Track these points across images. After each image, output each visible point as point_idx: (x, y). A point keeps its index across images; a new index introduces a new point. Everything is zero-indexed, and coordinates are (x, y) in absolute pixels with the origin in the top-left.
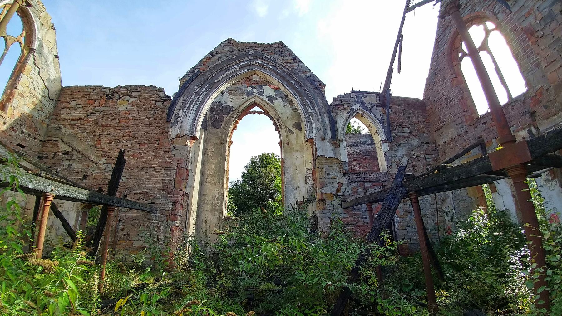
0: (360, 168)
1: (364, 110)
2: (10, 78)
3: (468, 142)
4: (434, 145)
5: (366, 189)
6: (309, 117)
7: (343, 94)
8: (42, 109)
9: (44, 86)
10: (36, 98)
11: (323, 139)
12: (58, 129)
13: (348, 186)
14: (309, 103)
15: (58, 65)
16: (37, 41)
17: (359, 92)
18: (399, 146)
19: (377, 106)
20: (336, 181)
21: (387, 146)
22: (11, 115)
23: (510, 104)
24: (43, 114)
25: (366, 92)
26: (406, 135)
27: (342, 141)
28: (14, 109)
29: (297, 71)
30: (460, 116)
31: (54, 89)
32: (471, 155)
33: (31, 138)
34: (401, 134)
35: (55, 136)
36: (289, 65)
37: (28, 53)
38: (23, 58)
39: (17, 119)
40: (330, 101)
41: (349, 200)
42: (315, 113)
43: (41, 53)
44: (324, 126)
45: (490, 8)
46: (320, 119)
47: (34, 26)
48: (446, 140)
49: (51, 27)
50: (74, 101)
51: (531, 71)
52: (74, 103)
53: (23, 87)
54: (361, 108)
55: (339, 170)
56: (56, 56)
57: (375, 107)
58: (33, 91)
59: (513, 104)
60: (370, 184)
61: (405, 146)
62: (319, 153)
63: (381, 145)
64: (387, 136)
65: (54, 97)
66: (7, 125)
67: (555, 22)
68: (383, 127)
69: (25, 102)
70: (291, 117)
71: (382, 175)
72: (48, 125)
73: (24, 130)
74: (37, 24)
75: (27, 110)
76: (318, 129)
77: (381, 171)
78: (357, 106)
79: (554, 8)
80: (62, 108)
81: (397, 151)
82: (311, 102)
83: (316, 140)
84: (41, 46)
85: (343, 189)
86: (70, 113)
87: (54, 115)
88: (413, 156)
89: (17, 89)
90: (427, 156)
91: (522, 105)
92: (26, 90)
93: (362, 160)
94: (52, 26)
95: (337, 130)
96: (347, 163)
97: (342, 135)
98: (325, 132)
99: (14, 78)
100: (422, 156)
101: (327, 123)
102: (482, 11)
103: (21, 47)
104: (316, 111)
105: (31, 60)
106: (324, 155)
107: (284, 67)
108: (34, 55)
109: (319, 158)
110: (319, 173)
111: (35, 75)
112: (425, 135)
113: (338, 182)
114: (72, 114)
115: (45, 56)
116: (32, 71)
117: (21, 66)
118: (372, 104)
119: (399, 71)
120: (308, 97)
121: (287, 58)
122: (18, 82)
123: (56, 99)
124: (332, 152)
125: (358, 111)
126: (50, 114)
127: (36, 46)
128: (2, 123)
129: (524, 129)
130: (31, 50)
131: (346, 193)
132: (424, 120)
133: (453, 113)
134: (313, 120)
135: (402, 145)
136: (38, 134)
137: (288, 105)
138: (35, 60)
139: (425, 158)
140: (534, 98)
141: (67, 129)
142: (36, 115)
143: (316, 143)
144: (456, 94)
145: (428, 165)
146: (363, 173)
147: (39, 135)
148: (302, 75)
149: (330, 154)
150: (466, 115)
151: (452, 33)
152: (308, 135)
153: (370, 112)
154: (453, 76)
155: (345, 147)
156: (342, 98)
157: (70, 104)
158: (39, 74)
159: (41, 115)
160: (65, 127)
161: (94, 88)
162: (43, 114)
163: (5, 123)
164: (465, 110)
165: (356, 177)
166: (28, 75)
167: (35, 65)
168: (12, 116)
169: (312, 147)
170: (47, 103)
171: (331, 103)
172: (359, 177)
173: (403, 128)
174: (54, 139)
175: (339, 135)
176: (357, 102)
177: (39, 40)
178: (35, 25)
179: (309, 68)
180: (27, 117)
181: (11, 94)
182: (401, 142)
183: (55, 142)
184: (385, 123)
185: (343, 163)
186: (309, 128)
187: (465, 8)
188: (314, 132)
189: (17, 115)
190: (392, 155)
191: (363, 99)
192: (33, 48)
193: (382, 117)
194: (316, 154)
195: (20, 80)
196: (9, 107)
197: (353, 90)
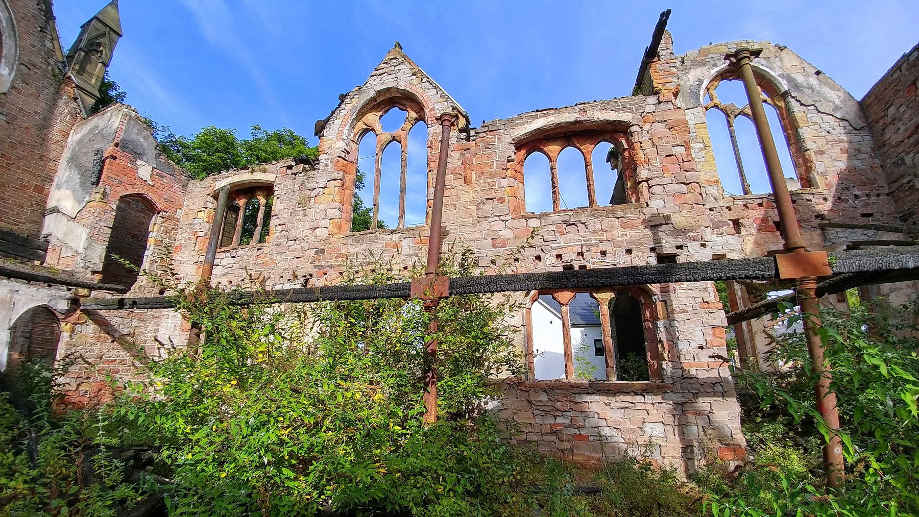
2: (789, 145)
8: (860, 151)
9: (838, 120)
10: (841, 142)
12: (900, 163)
15: (830, 81)
16: (780, 79)
22: (827, 185)
24: (865, 156)
28: (824, 175)
31: (851, 111)
33: (873, 198)
35: (903, 176)
37: (785, 102)
38: (784, 112)
39: (838, 185)
43: (797, 87)
47: (761, 69)
49: (779, 51)
50: (889, 107)
52: (892, 111)
53: (815, 142)
56: (818, 73)
58: (829, 137)
65: (861, 124)
66: (830, 199)
69: (831, 157)
72: (882, 166)
73: (857, 193)
74: (762, 65)
75: (842, 165)
80: (883, 130)
84: (790, 80)
86: (899, 129)
87: (879, 146)
89: (809, 150)
92: (821, 143)
94: (779, 48)
99: (793, 141)
103: (769, 104)
105: (795, 106)
108: (793, 97)
111: (816, 118)
114: (903, 128)
115: (805, 85)
116: (809, 116)
117: (789, 122)
122: (804, 141)
123: (865, 125)
126: (873, 149)
127: (784, 86)
128: (822, 201)
130: (785, 95)
136: (878, 187)
138: (799, 101)
141: (911, 155)
142: (857, 163)
147: (882, 187)
157: (889, 116)
158: (819, 112)
159: (863, 159)
160: (908, 154)
161: (898, 67)
162: (865, 156)
163: (825, 199)
166: (808, 125)
167: (805, 106)
168: (828, 186)
170: (859, 138)
174: (905, 180)
177: (779, 76)
178: (761, 67)
180: (849, 173)
181: (806, 161)
183: (909, 185)
189: (834, 181)
192: (783, 91)
195: (802, 137)
196: (817, 177)
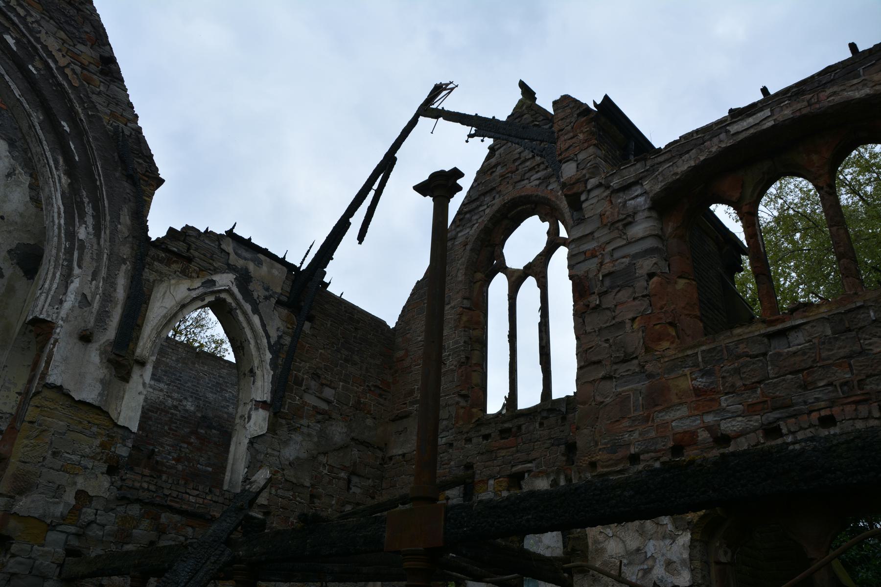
0: (178, 460)
1: (239, 296)
3: (445, 469)
4: (380, 454)
5: (161, 531)
6: (69, 252)
7: (202, 230)
11: (86, 338)
13: (107, 510)
14: (89, 209)
17: (247, 244)
18: (295, 429)
19: (279, 303)
20: (75, 483)
21: (265, 419)
23: (540, 412)
25: (265, 252)
26: (324, 406)
27: (142, 364)
29: (94, 98)
34: (311, 400)
36: (78, 69)
40: (156, 230)
41: (95, 552)
42: (95, 246)
44: (108, 298)
46: (103, 273)
54: (235, 290)
55: (98, 450)
57: (273, 301)
59: (545, 414)
60: (177, 518)
61: (309, 435)
62: (54, 377)
63: (249, 413)
64: (274, 392)
67: (631, 290)
68: (274, 364)
70: (18, 219)
71: (221, 500)
76: (84, 301)
77: (225, 487)
78: (225, 280)
79: (640, 262)
81: (286, 443)
82: (96, 208)
83: (61, 332)
85: (88, 513)
88: (321, 469)
90: (355, 479)
91: (560, 421)
93: (193, 440)
95: (140, 327)
96: (132, 436)
97: (149, 345)
98: (103, 317)
100: (343, 475)
101: (120, 293)
104: (99, 244)
106: (69, 386)
107: (61, 69)
109: (47, 393)
110: (26, 442)
112: (369, 422)
113: (79, 486)
118: (267, 289)
119: (361, 238)
120: (94, 191)
121: (80, 47)
124: (98, 388)
125: (223, 295)
129: (548, 475)
131: (95, 531)
132: (379, 383)
134: (80, 267)
135: (305, 430)
137: (25, 180)
139: (349, 481)
143: (56, 341)
145: (349, 503)
146: (170, 481)
148: (106, 119)
149: (89, 394)
150: (461, 404)
151: (495, 208)
152: (40, 306)
153: (256, 311)
154: (466, 303)
155: (144, 384)
156: (194, 239)
164: (463, 392)
165: (145, 485)
169: (41, 349)
171: (158, 239)
172: (152, 488)
173: (322, 385)
175: (141, 344)
176: (231, 268)
179: (137, 111)
182: (304, 422)
184: (283, 356)
185: (120, 431)
186: (55, 286)
187: (534, 172)
188: (67, 305)
190: (269, 451)
191: (251, 267)
193: (280, 337)
194: (44, 375)
197: (235, 231)
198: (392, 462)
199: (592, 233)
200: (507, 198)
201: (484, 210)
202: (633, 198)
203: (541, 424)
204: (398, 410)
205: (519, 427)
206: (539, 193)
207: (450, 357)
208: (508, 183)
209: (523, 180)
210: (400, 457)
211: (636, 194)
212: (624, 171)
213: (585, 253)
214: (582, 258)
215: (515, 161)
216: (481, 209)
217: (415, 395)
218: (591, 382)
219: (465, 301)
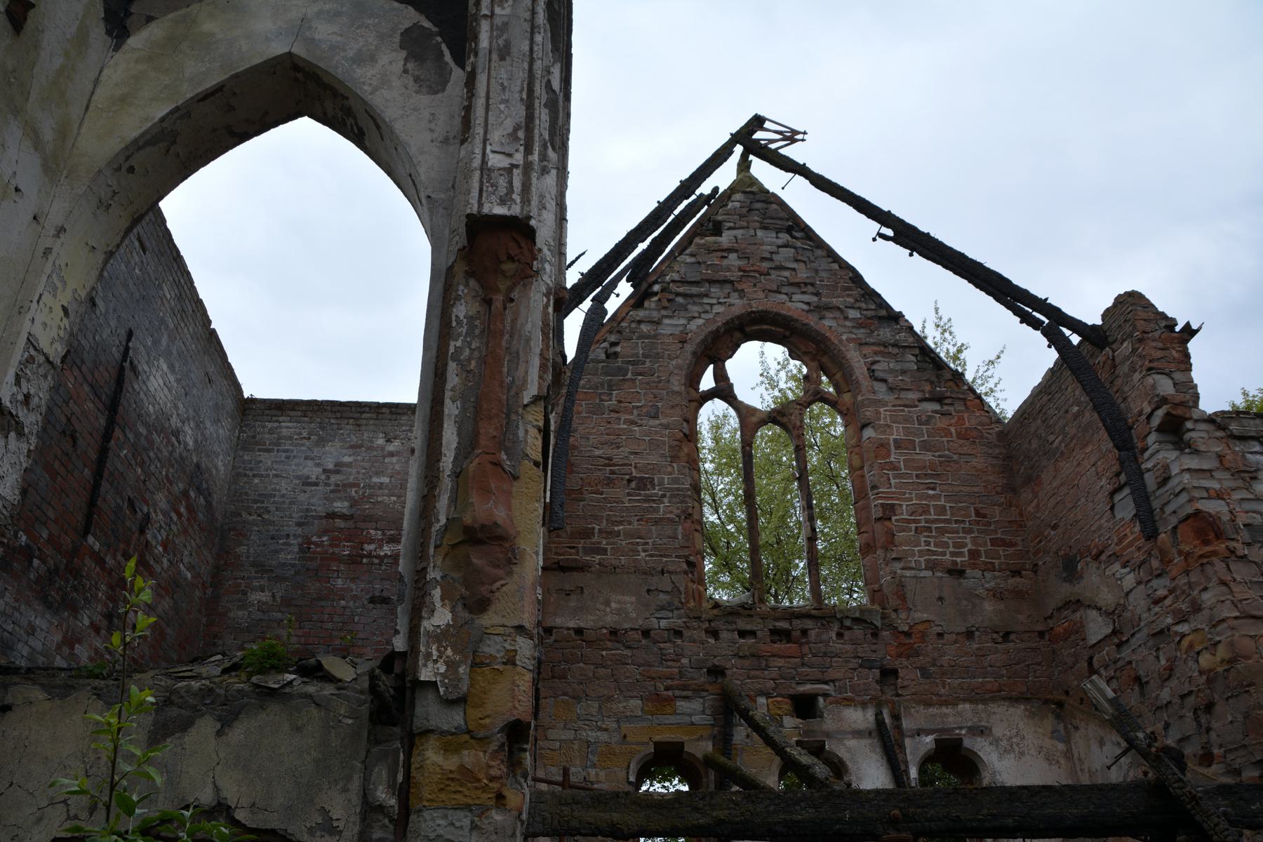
23: (841, 621)
30: (671, 568)
32: (672, 719)
45: (867, 350)
48: (586, 621)
51: (912, 569)
59: (848, 623)
102: (844, 337)
133: (647, 543)
140: (902, 637)
144: (678, 489)
164: (692, 558)
198: (553, 638)
199: (1210, 471)
200: (756, 306)
201: (712, 305)
202: (1251, 453)
203: (840, 635)
204: (556, 553)
205: (805, 632)
206: (812, 324)
207: (666, 500)
208: (755, 285)
209: (780, 293)
210: (572, 632)
211: (1255, 449)
212: (1244, 420)
213: (1207, 490)
214: (1205, 495)
215: (763, 259)
216: (706, 300)
217: (596, 539)
218: (1251, 637)
219: (685, 424)
